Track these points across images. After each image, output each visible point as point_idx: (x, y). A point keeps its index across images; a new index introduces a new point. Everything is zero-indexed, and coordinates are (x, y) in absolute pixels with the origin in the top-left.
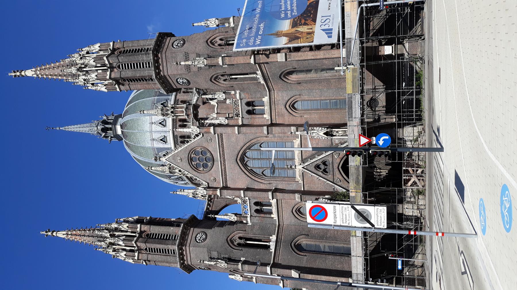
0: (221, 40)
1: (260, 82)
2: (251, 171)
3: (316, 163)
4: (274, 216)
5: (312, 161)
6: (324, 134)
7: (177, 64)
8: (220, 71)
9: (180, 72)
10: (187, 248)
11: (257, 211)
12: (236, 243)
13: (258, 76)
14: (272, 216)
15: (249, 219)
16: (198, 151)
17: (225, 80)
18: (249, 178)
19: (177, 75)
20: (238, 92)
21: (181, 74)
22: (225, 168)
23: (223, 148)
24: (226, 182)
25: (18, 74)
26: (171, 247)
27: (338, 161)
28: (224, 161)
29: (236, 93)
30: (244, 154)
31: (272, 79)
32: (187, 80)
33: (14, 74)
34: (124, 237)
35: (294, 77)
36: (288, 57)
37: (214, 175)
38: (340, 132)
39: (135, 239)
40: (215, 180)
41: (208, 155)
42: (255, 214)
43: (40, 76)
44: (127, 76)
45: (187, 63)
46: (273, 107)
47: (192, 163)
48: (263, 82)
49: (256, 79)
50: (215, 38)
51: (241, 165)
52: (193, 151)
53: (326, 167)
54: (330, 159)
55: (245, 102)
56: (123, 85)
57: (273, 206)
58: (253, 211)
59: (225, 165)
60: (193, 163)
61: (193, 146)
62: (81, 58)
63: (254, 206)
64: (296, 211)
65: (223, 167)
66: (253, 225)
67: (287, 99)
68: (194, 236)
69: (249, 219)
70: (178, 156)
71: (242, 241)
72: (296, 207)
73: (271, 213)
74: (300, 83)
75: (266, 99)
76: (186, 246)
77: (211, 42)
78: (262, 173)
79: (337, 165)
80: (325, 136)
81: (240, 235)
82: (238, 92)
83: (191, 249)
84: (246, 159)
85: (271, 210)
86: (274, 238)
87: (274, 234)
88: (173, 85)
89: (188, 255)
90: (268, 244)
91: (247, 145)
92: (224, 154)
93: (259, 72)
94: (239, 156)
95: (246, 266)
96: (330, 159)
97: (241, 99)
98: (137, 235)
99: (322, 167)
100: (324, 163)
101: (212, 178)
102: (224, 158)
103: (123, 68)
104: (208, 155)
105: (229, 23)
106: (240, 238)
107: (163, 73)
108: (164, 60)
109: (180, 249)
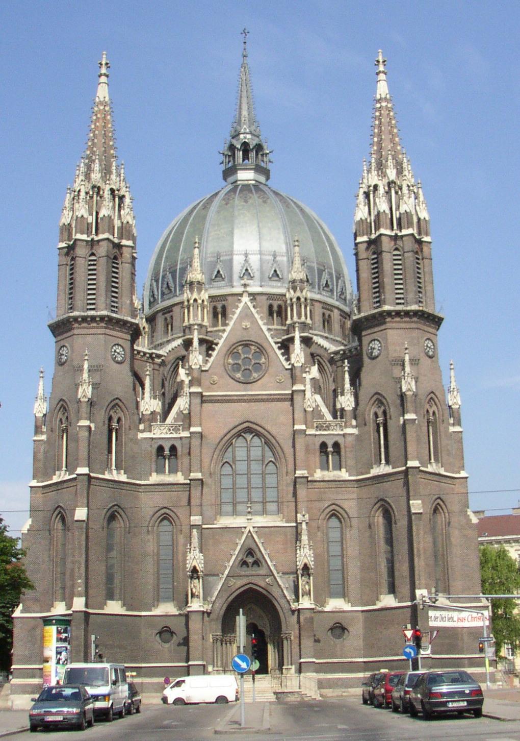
0: (434, 413)
1: (372, 468)
2: (230, 444)
3: (257, 551)
4: (154, 478)
5: (260, 545)
6: (305, 565)
7: (406, 349)
8: (393, 411)
9: (390, 348)
10: (103, 331)
11: (160, 449)
12: (111, 413)
13: (382, 466)
14: (154, 474)
16: (260, 359)
17: (376, 415)
18: (218, 441)
19: (386, 343)
20: (355, 431)
21: (387, 348)
23: (267, 400)
24: (211, 401)
26: (102, 301)
27: (263, 584)
28: (245, 401)
29: (353, 427)
32: (376, 357)
34: (112, 218)
35: (379, 519)
38: (307, 587)
39: (111, 237)
40: (214, 383)
42: (156, 446)
43: (378, 105)
44: (385, 262)
46: (331, 485)
47: (240, 345)
50: (436, 404)
52: (261, 350)
53: (250, 565)
54: (263, 571)
55: (340, 441)
56: (367, 249)
57: (172, 475)
58: (160, 443)
60: (240, 348)
61: (269, 350)
62: (408, 186)
64: (165, 513)
66: (136, 441)
68: (120, 342)
70: (252, 323)
71: (115, 425)
73: (160, 470)
75: (344, 475)
76: (105, 328)
77: (432, 398)
78: (226, 462)
79: (253, 581)
80: (302, 566)
81: (123, 419)
83: (101, 336)
84: (249, 437)
86: (123, 478)
87: (128, 478)
88: (369, 331)
90: (114, 467)
91: (273, 441)
93: (388, 469)
94: (254, 426)
95: (87, 434)
97: (344, 435)
98: (116, 241)
99: (250, 560)
100: (257, 563)
101: (216, 378)
103: (394, 255)
104: (255, 375)
105: (453, 425)
106: (119, 420)
107: (390, 322)
108: (408, 326)
109: (102, 318)
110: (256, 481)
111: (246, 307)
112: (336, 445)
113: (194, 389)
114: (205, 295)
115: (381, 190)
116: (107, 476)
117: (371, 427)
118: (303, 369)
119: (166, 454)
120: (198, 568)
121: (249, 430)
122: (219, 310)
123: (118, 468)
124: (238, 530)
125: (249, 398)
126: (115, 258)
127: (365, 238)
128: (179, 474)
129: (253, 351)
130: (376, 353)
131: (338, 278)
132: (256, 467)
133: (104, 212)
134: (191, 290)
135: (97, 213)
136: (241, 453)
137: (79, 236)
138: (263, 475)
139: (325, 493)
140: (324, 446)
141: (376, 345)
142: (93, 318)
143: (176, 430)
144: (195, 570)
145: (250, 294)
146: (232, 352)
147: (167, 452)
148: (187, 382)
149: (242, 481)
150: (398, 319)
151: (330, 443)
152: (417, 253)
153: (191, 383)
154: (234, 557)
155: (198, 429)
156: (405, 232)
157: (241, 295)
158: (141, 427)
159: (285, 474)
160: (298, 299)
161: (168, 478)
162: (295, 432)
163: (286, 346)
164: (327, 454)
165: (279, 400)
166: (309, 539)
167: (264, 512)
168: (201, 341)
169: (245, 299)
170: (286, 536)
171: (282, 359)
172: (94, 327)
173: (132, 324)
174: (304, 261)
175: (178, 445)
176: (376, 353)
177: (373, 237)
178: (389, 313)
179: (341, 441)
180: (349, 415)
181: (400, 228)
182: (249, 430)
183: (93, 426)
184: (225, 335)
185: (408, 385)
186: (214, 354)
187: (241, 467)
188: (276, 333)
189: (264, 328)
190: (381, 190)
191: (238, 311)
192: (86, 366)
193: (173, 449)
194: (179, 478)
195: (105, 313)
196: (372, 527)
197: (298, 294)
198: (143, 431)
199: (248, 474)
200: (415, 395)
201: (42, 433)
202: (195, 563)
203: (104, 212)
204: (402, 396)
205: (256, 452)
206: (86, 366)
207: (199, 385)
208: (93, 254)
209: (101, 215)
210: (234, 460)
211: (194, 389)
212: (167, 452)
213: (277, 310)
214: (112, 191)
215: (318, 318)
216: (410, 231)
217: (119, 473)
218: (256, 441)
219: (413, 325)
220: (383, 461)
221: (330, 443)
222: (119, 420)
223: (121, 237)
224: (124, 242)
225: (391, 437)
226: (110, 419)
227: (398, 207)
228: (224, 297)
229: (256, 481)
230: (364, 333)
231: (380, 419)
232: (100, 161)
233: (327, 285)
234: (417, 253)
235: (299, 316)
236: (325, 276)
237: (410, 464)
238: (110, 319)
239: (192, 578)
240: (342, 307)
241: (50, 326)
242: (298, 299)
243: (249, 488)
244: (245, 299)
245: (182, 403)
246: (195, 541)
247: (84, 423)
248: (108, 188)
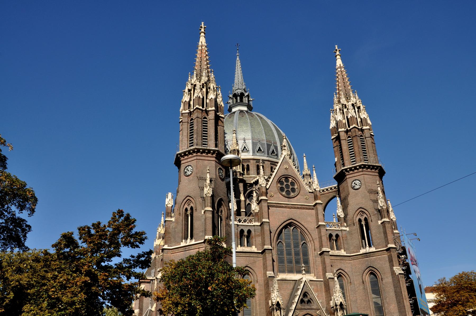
2: (281, 232)
6: (341, 302)
13: (368, 248)
22: (282, 207)
23: (301, 208)
25: (203, 30)
28: (289, 208)
29: (346, 227)
31: (367, 260)
33: (203, 27)
35: (367, 278)
36: (401, 275)
37: (275, 196)
42: (239, 229)
46: (338, 258)
49: (186, 238)
51: (287, 222)
53: (306, 302)
58: (242, 228)
59: (286, 207)
60: (284, 179)
63: (247, 230)
65: (283, 205)
67: (346, 271)
72: (251, 270)
74: (363, 283)
75: (342, 252)
79: (310, 313)
82: (347, 229)
85: (244, 246)
91: (306, 231)
92: (295, 208)
96: (314, 307)
97: (341, 230)
99: (306, 300)
102: (292, 208)
108: (373, 174)
117: (357, 226)
120: (280, 303)
121: (290, 224)
125: (291, 206)
128: (254, 247)
129: (290, 181)
139: (335, 262)
144: (278, 304)
151: (334, 235)
154: (298, 297)
159: (313, 250)
170: (317, 286)
172: (208, 157)
179: (340, 234)
180: (343, 220)
196: (365, 283)
202: (278, 300)
208: (205, 118)
220: (367, 245)
221: (334, 235)
230: (348, 177)
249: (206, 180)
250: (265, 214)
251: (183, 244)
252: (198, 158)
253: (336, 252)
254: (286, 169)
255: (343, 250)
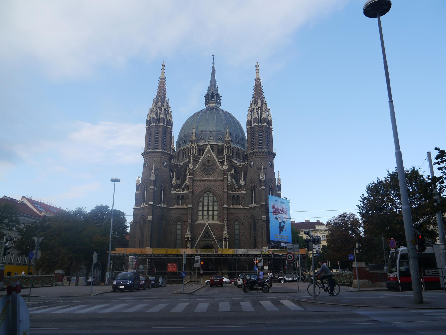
4: (176, 206)
11: (179, 196)
14: (176, 205)
15: (174, 192)
17: (252, 186)
20: (245, 192)
22: (203, 181)
23: (215, 181)
26: (160, 146)
28: (208, 181)
29: (244, 191)
30: (211, 192)
32: (252, 167)
41: (211, 172)
45: (262, 169)
48: (250, 206)
52: (214, 163)
54: (211, 239)
59: (205, 181)
68: (166, 160)
69: (174, 192)
71: (163, 188)
73: (178, 204)
75: (240, 207)
82: (245, 192)
86: (165, 206)
89: (156, 156)
92: (211, 181)
93: (256, 205)
98: (165, 126)
106: (164, 187)
109: (160, 152)
110: (210, 208)
111: (209, 149)
112: (238, 196)
113: (191, 177)
114: (196, 145)
115: (256, 110)
116: (159, 206)
118: (227, 170)
119: (180, 199)
122: (201, 150)
123: (163, 203)
124: (204, 225)
126: (165, 132)
127: (250, 127)
128: (185, 205)
130: (252, 165)
131: (242, 140)
132: (211, 204)
133: (162, 116)
134: (192, 143)
135: (159, 116)
136: (206, 199)
137: (152, 124)
138: (213, 206)
140: (234, 196)
141: (252, 163)
142: (157, 152)
143: (184, 190)
145: (210, 145)
146: (203, 164)
147: (180, 198)
148: (188, 174)
149: (205, 208)
150: (260, 154)
151: (236, 196)
152: (267, 132)
153: (190, 175)
155: (191, 190)
156: (263, 125)
157: (207, 145)
158: (172, 189)
160: (228, 146)
161: (180, 207)
162: (224, 192)
163: (222, 163)
164: (235, 199)
165: (219, 181)
166: (227, 229)
167: (213, 219)
168: (194, 160)
169: (209, 147)
171: (220, 167)
173: (170, 154)
174: (230, 134)
175: (184, 195)
176: (252, 165)
177: (252, 126)
178: (257, 152)
181: (261, 123)
182: (208, 191)
183: (155, 188)
184: (201, 159)
185: (262, 177)
186: (198, 165)
187: (206, 203)
188: (219, 159)
189: (215, 157)
190: (256, 110)
191: (206, 151)
192: (153, 168)
193: (183, 196)
194: (185, 206)
195: (161, 150)
197: (228, 145)
198: (172, 191)
199: (208, 206)
200: (265, 180)
201: (138, 190)
203: (162, 116)
204: (260, 181)
205: (211, 198)
206: (153, 168)
207: (192, 175)
208: (157, 130)
209: (160, 117)
210: (203, 201)
211: (191, 177)
212: (180, 198)
213: (220, 150)
214: (164, 109)
215: (235, 153)
216: (265, 124)
217: (164, 204)
218: (211, 195)
219: (265, 156)
221: (236, 196)
222: (164, 187)
223: (167, 125)
224: (168, 126)
225: (257, 195)
226: (161, 186)
227: (261, 117)
228: (203, 146)
229: (210, 208)
231: (253, 188)
232: (161, 98)
233: (238, 142)
234: (267, 132)
235: (228, 153)
236: (238, 140)
237: (262, 203)
238: (162, 152)
239: (187, 241)
240: (243, 150)
241: (142, 154)
242: (228, 146)
243: (208, 210)
244: (209, 147)
245: (187, 181)
246: (188, 228)
247: (153, 187)
248: (163, 108)
249: (155, 169)
250: (190, 187)
251: (142, 206)
252: (151, 156)
253: (236, 207)
254: (209, 157)
255: (240, 205)
